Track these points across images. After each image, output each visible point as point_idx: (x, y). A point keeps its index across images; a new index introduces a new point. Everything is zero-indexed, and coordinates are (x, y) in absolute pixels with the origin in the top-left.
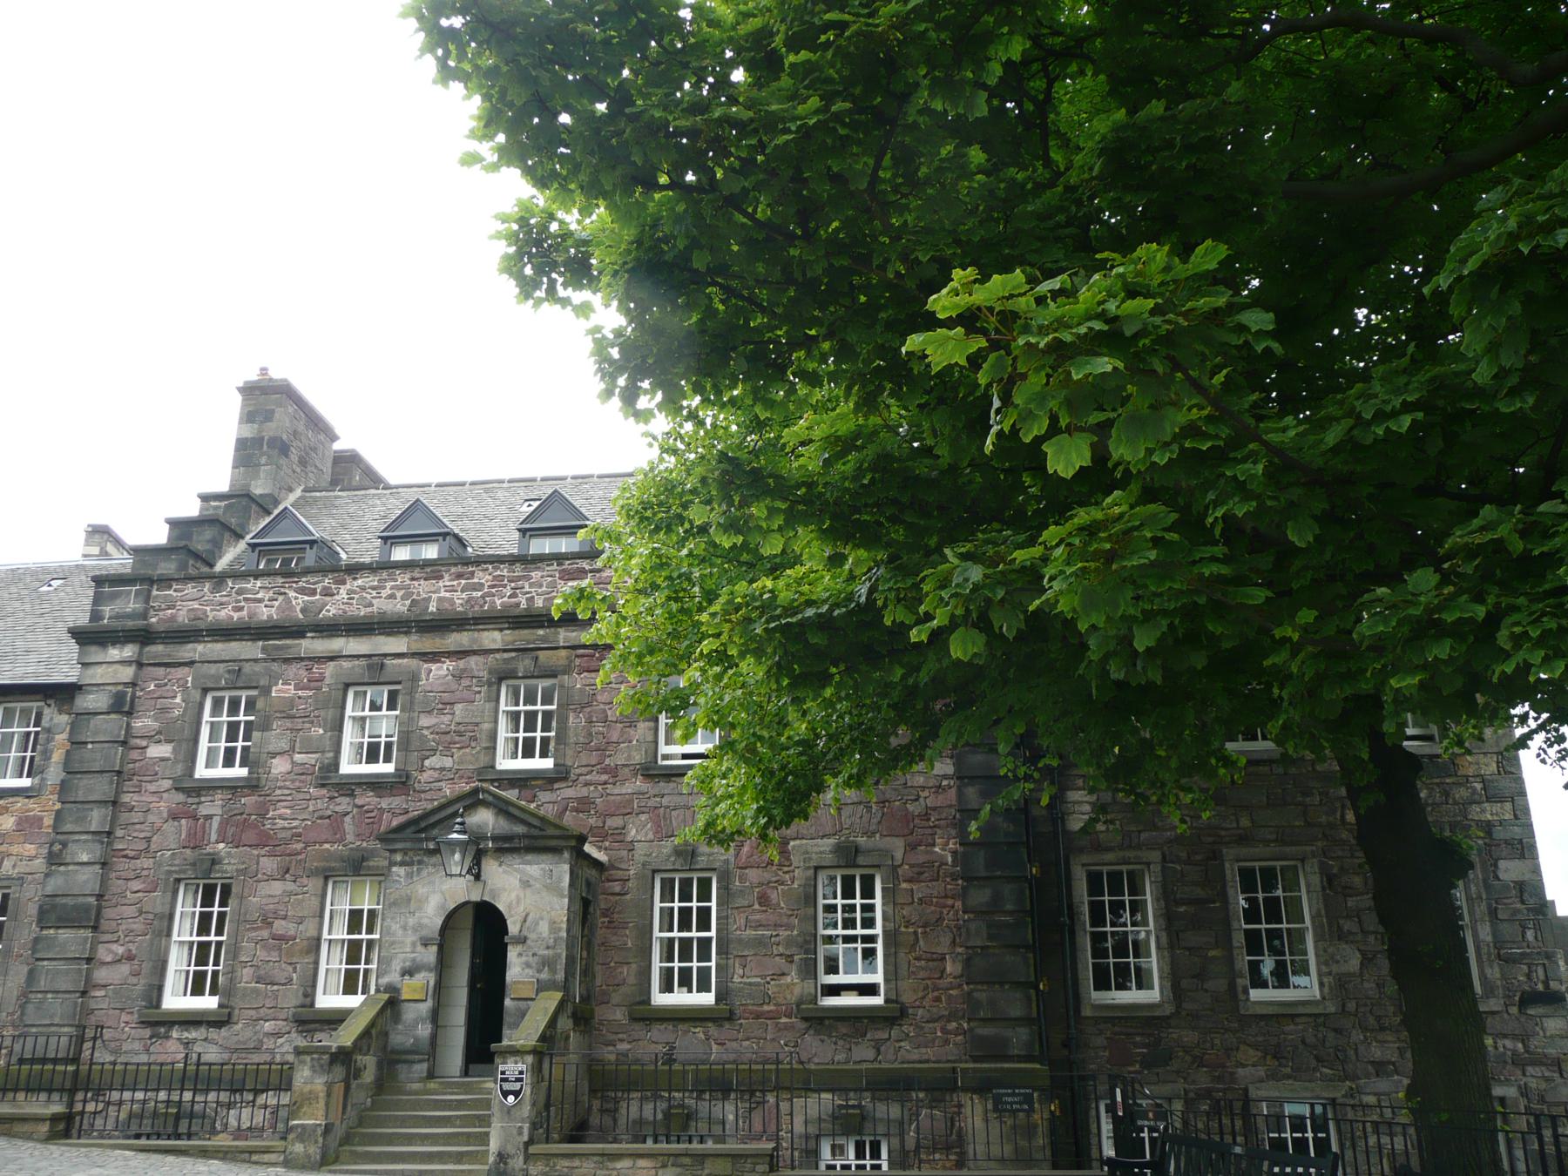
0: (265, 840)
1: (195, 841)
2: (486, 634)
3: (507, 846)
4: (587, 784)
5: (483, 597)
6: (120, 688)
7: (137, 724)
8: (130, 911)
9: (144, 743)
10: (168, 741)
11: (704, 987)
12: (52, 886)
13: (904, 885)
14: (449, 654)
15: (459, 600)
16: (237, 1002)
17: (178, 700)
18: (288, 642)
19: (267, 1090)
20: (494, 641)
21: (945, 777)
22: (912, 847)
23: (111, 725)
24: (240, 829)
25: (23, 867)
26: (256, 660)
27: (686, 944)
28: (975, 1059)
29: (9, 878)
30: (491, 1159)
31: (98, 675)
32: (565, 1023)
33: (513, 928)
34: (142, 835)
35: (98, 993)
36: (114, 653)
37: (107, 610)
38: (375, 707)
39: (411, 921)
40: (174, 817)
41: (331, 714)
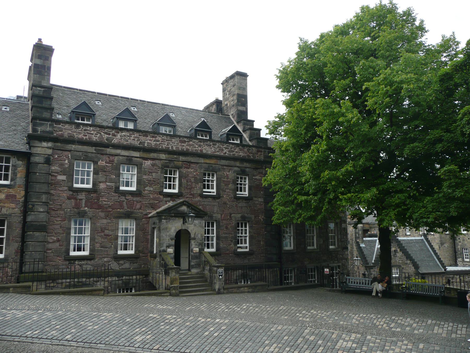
0: (100, 207)
1: (77, 206)
2: (161, 155)
4: (187, 198)
5: (159, 144)
6: (46, 156)
8: (58, 227)
9: (56, 175)
10: (64, 175)
17: (66, 162)
18: (103, 149)
19: (108, 277)
20: (163, 157)
21: (262, 202)
22: (255, 217)
23: (43, 168)
24: (90, 204)
25: (10, 211)
26: (92, 153)
29: (6, 215)
30: (217, 290)
33: (192, 236)
34: (59, 204)
35: (49, 252)
36: (45, 144)
37: (39, 129)
39: (168, 234)
40: (69, 198)
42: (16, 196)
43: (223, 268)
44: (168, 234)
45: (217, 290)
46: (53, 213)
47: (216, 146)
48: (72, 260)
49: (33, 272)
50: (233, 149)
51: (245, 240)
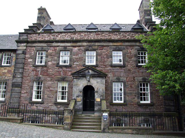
1: (37, 75)
3: (93, 76)
4: (101, 68)
7: (26, 56)
8: (27, 85)
11: (121, 100)
12: (14, 81)
13: (153, 85)
14: (77, 46)
15: (79, 38)
16: (45, 100)
17: (33, 52)
20: (85, 44)
23: (22, 56)
25: (9, 78)
26: (45, 46)
28: (165, 111)
30: (102, 129)
31: (20, 48)
33: (96, 90)
36: (23, 45)
37: (21, 38)
39: (78, 88)
42: (11, 70)
43: (108, 112)
44: (78, 88)
45: (102, 129)
46: (25, 78)
47: (121, 35)
48: (33, 103)
50: (133, 35)
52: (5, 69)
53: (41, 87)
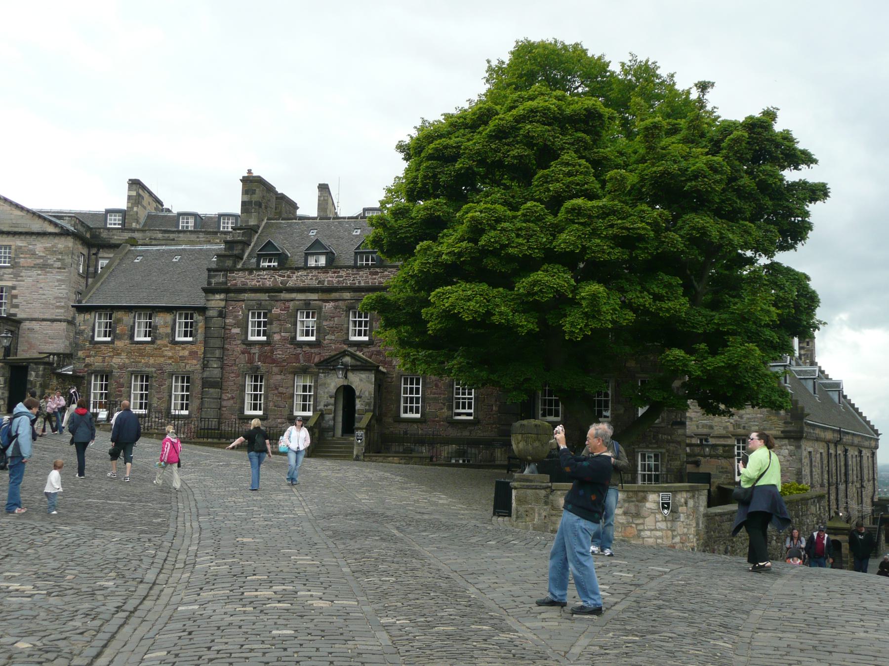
0: (274, 361)
1: (251, 361)
3: (355, 369)
7: (227, 321)
11: (417, 412)
12: (206, 374)
14: (332, 300)
16: (269, 413)
23: (218, 321)
24: (264, 358)
27: (412, 399)
32: (373, 422)
33: (357, 393)
36: (217, 296)
37: (213, 281)
38: (308, 317)
40: (243, 353)
41: (293, 320)
46: (228, 368)
49: (208, 429)
51: (470, 404)
52: (184, 349)
53: (261, 386)
